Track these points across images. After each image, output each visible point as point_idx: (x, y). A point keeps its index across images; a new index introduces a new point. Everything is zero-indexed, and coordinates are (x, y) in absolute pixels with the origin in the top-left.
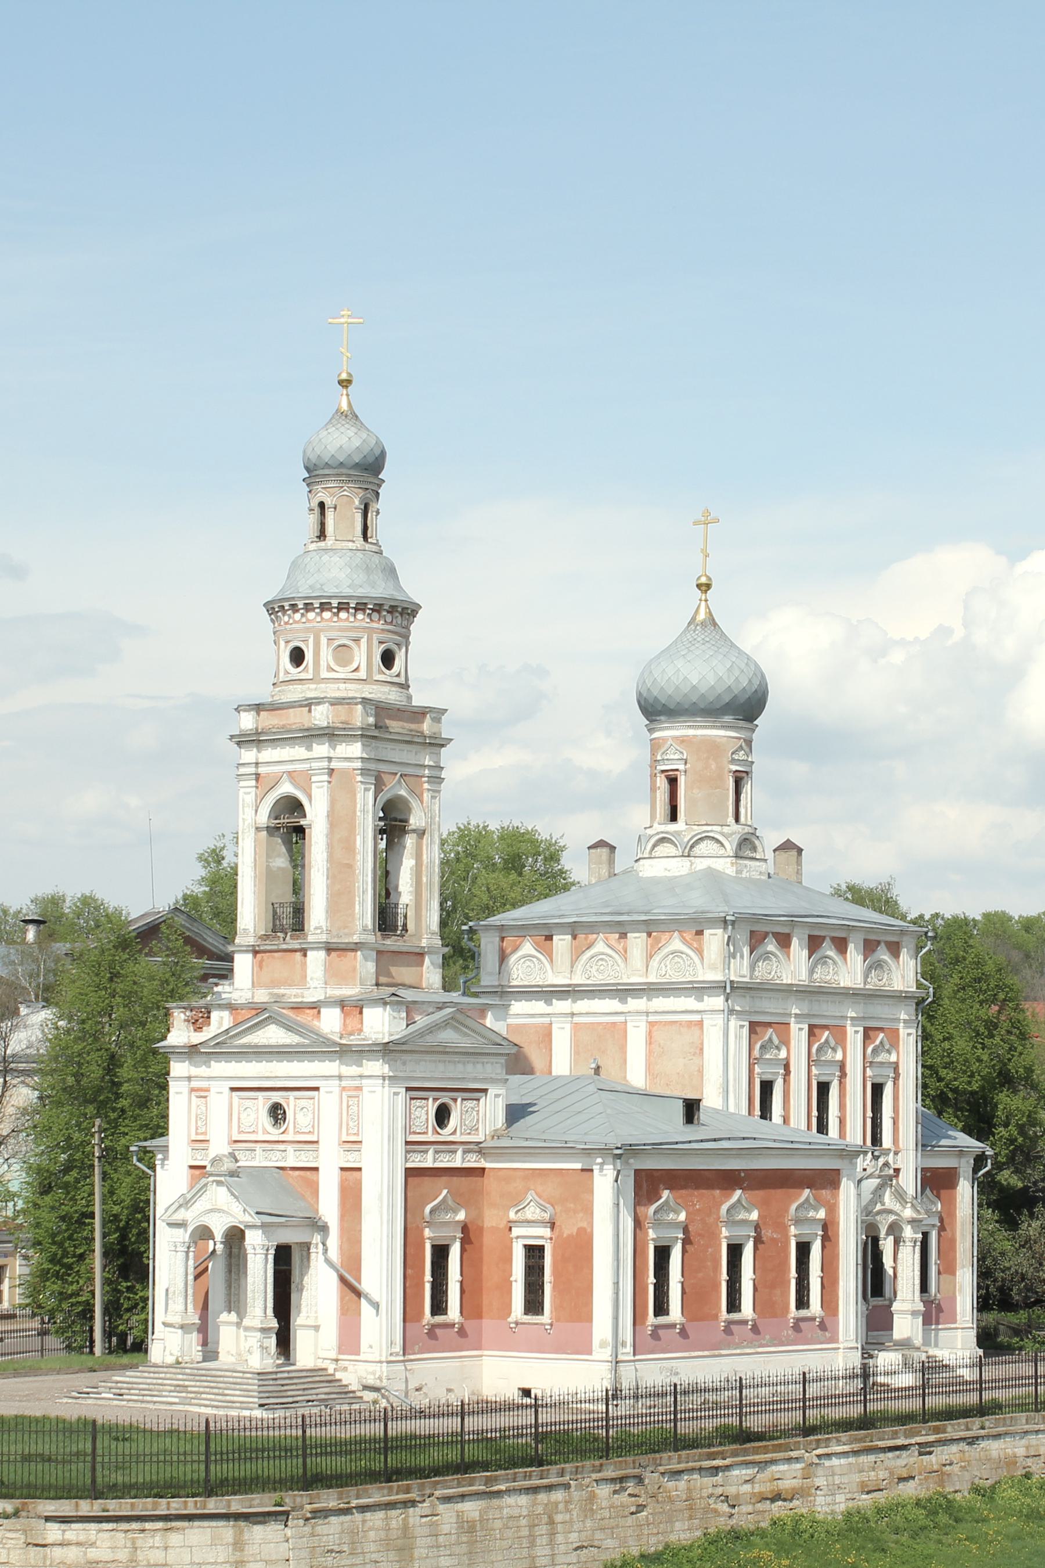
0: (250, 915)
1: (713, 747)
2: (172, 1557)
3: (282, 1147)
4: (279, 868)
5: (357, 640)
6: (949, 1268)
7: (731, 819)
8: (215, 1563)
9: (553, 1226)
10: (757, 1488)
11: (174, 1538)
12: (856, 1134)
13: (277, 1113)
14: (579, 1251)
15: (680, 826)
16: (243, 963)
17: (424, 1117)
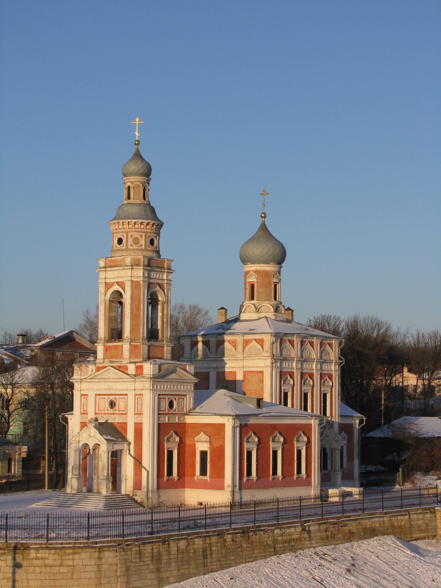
0: (102, 332)
2: (75, 563)
3: (114, 416)
4: (113, 316)
5: (141, 236)
6: (351, 459)
7: (273, 299)
8: (91, 565)
9: (210, 442)
10: (284, 538)
11: (77, 556)
12: (317, 411)
13: (112, 404)
14: (219, 453)
15: (255, 302)
16: (100, 349)
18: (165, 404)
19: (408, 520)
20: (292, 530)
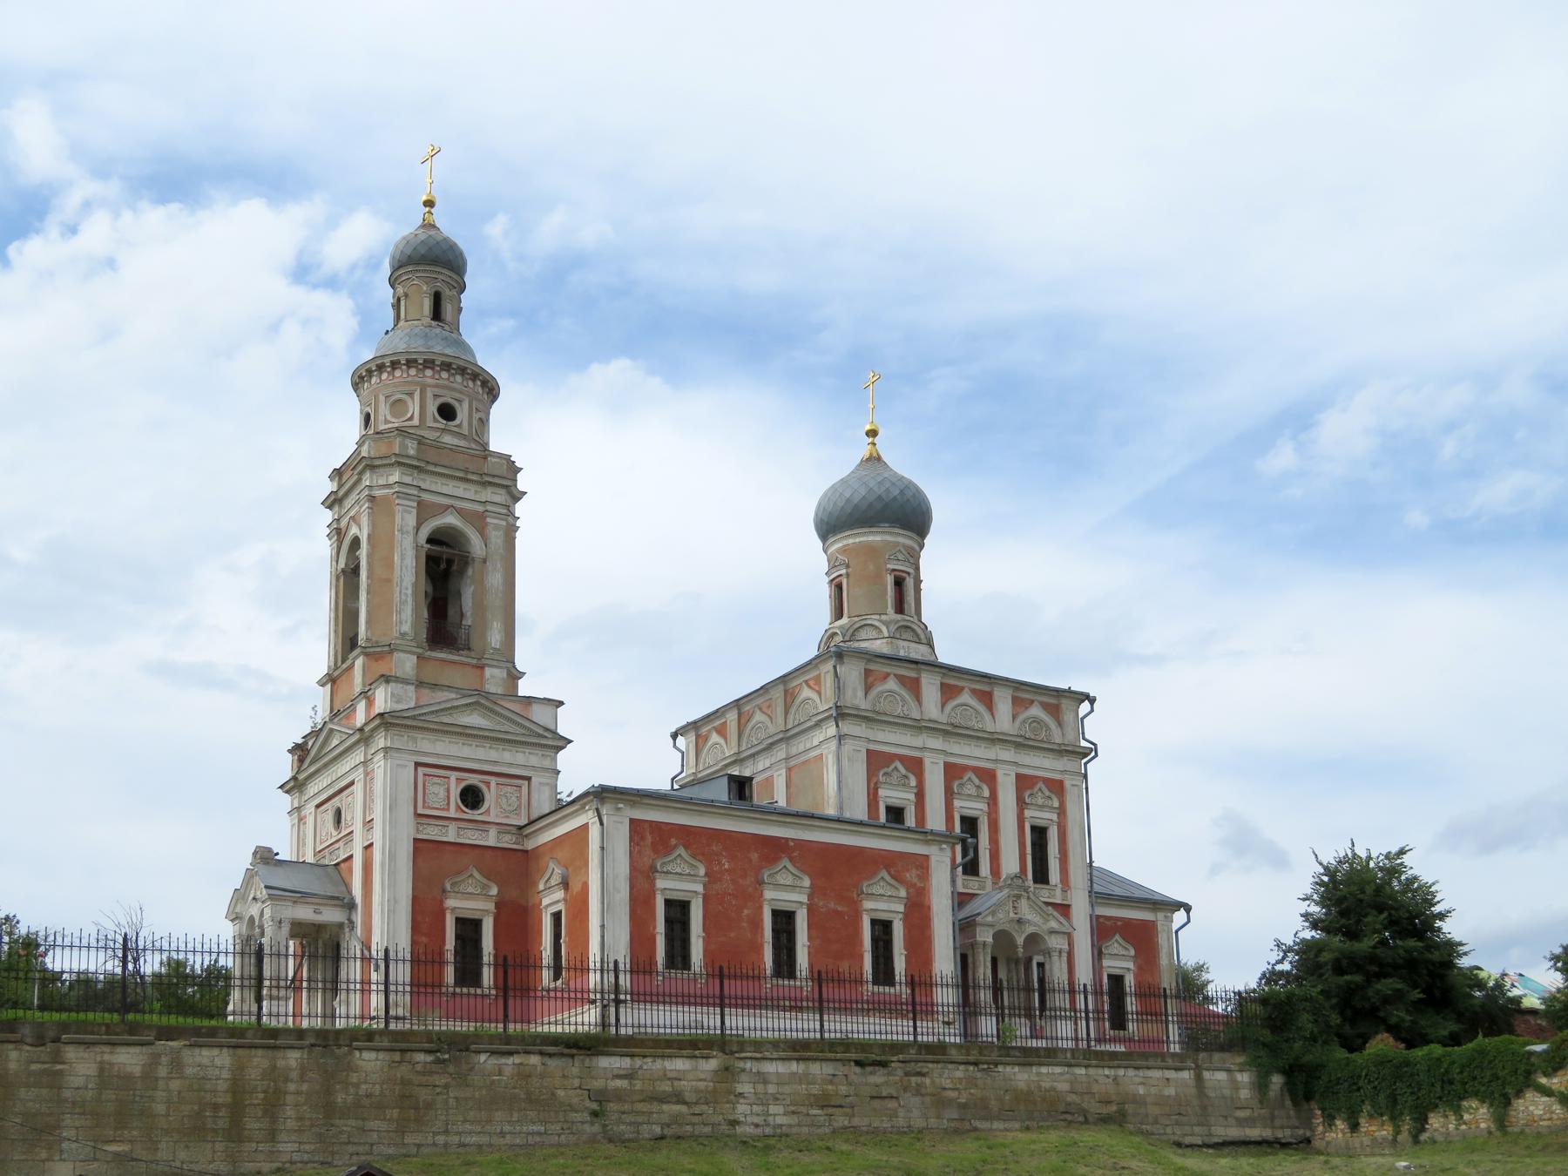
1: (871, 551)
7: (890, 610)
15: (844, 621)
17: (442, 794)
18: (444, 795)
19: (1192, 1083)
20: (680, 1064)
